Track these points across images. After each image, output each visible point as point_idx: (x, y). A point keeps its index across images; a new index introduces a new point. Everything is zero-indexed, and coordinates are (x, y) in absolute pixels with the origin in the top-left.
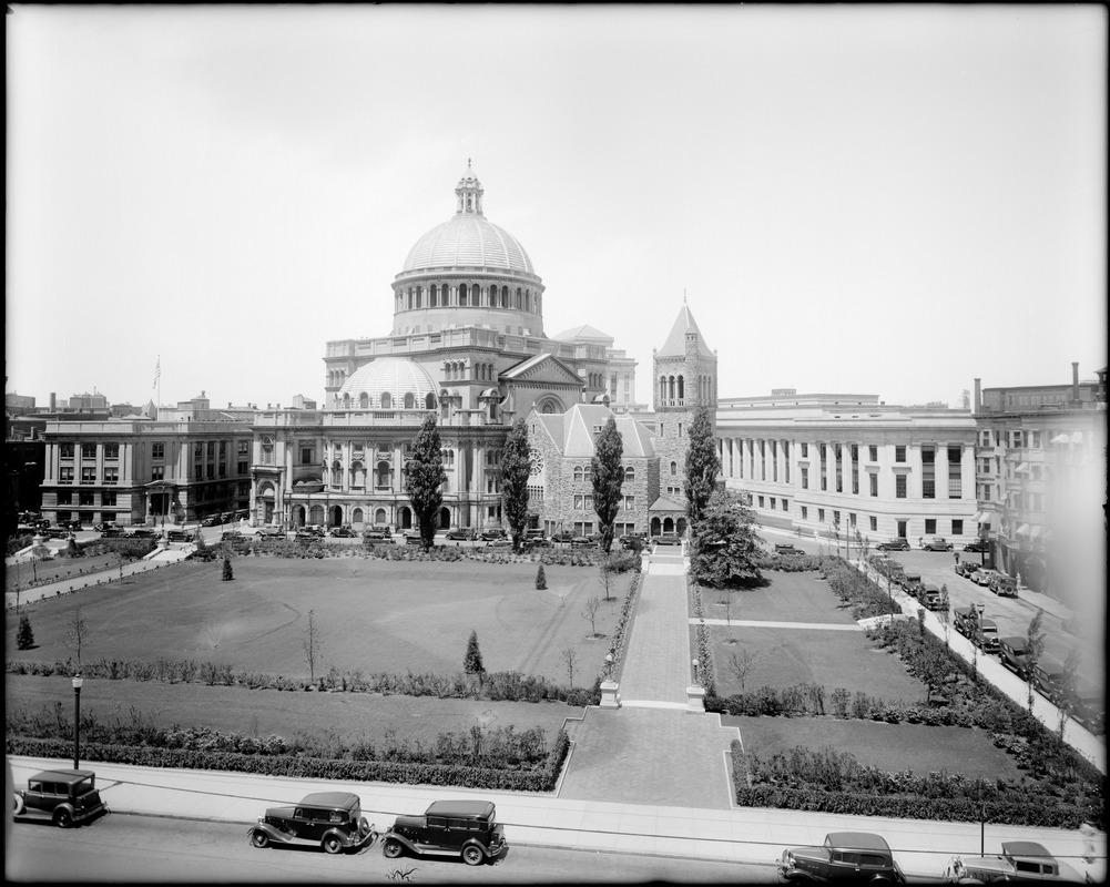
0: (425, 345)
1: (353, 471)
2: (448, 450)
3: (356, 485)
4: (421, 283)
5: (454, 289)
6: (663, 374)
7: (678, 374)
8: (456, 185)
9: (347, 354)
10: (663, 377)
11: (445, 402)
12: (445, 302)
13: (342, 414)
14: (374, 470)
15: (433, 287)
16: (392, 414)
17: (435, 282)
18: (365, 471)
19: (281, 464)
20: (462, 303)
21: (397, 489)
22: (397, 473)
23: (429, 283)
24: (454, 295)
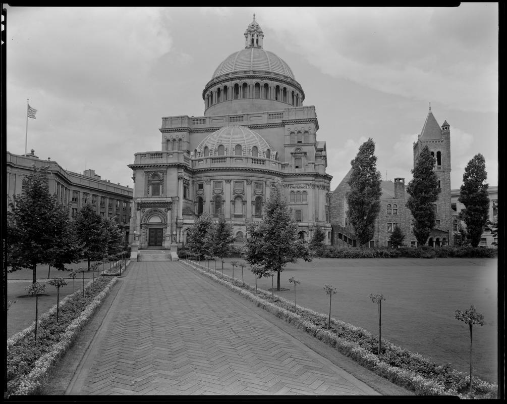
0: (265, 120)
1: (233, 202)
2: (301, 190)
3: (235, 214)
4: (248, 81)
5: (272, 88)
7: (438, 150)
8: (245, 31)
9: (186, 125)
12: (266, 98)
13: (223, 159)
14: (252, 202)
16: (262, 162)
18: (244, 202)
19: (174, 195)
23: (255, 81)
24: (272, 92)
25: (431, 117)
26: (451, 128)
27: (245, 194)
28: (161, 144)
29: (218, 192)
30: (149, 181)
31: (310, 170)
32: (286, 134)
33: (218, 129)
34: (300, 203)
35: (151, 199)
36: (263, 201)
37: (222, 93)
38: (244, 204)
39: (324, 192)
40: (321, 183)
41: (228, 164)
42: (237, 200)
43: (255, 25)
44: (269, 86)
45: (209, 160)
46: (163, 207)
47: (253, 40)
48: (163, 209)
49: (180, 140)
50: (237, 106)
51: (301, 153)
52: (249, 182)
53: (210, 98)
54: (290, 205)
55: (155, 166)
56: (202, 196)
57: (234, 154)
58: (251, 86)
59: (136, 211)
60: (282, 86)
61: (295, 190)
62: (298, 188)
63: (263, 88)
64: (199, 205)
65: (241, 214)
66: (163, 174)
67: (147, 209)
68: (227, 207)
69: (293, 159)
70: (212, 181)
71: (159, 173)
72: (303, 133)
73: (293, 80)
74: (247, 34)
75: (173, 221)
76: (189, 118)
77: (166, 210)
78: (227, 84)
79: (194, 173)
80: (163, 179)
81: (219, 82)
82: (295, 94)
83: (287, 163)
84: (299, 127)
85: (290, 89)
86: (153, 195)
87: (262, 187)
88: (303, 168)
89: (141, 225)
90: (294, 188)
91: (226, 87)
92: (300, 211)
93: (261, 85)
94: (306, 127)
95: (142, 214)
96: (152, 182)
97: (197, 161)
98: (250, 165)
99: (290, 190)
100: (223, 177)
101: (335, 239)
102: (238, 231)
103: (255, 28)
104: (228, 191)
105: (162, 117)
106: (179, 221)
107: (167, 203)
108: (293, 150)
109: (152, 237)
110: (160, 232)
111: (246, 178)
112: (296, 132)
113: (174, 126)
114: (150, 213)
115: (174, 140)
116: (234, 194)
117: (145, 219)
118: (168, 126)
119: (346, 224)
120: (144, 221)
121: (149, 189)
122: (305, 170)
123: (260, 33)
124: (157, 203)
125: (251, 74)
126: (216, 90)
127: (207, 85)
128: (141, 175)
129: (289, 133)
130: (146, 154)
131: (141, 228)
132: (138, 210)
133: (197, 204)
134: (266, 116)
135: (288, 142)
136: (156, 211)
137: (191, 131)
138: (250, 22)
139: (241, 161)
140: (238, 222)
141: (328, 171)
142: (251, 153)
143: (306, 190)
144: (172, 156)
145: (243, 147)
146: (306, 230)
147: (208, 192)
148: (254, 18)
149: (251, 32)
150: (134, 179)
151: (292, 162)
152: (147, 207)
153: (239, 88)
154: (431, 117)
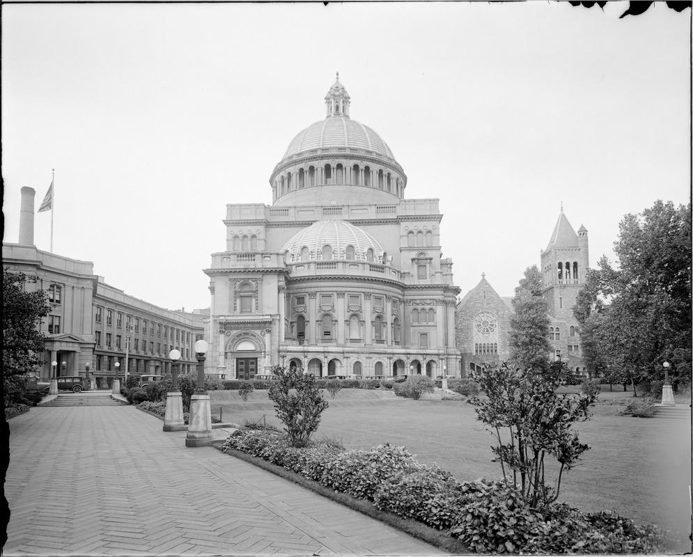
0: (372, 214)
1: (347, 322)
2: (427, 307)
4: (344, 162)
5: (375, 172)
6: (559, 261)
7: (574, 261)
9: (262, 217)
10: (560, 265)
11: (422, 263)
14: (372, 322)
15: (356, 167)
17: (358, 162)
20: (381, 188)
21: (390, 343)
22: (389, 325)
23: (352, 163)
24: (374, 177)
25: (563, 215)
26: (589, 234)
27: (363, 311)
28: (226, 242)
29: (327, 309)
30: (236, 292)
31: (438, 281)
32: (402, 234)
33: (309, 224)
34: (424, 324)
35: (240, 318)
36: (384, 321)
37: (307, 176)
38: (362, 325)
39: (452, 310)
40: (450, 299)
41: (339, 271)
42: (352, 320)
43: (340, 87)
44: (371, 169)
45: (312, 266)
46: (254, 328)
47: (337, 108)
48: (258, 332)
49: (254, 236)
50: (332, 193)
51: (426, 259)
52: (368, 295)
53: (286, 181)
54: (412, 326)
55: (246, 271)
56: (303, 313)
57: (345, 258)
58: (348, 169)
59: (218, 334)
60: (386, 171)
61: (419, 307)
62: (423, 305)
63: (363, 172)
64: (298, 326)
65: (358, 338)
66: (257, 283)
67: (234, 332)
68: (340, 330)
69: (416, 266)
70: (318, 294)
71: (250, 281)
72: (424, 233)
73: (396, 163)
74: (329, 99)
75: (273, 347)
76: (265, 207)
77: (263, 333)
78: (315, 163)
79: (290, 282)
80: (257, 290)
81: (302, 161)
82: (399, 181)
83: (408, 271)
84: (420, 225)
85: (394, 175)
86: (241, 312)
87: (382, 304)
88: (428, 279)
89: (226, 353)
90: (417, 304)
91: (312, 169)
92: (426, 334)
93: (360, 167)
94: (428, 225)
95: (227, 339)
96: (241, 294)
97: (294, 267)
98: (367, 273)
99: (412, 307)
100: (335, 289)
101: (466, 370)
102: (355, 361)
103: (341, 91)
104: (341, 308)
105: (226, 204)
106: (281, 348)
107: (265, 323)
108: (414, 254)
109: (242, 370)
110: (252, 363)
111: (363, 290)
112: (415, 232)
113: (244, 218)
114: (238, 337)
115: (245, 236)
116: (348, 312)
117: (230, 346)
118: (236, 217)
119: (477, 351)
120: (230, 348)
121: (235, 304)
122: (431, 281)
123: (346, 100)
124: (241, 323)
125: (348, 152)
126: (298, 171)
127: (279, 164)
128: (223, 287)
129: (406, 233)
130: (230, 255)
131: (226, 358)
132: (221, 332)
133: (295, 325)
134: (374, 209)
135: (404, 245)
136: (248, 333)
137: (268, 225)
138: (332, 82)
139: (356, 267)
140: (356, 350)
141: (456, 283)
142: (366, 257)
143: (434, 307)
144: (268, 259)
145: (356, 249)
146: (435, 358)
147: (312, 309)
148: (338, 78)
149: (335, 96)
150: (212, 289)
151: (414, 270)
152: (235, 329)
153: (332, 170)
154: (563, 218)
